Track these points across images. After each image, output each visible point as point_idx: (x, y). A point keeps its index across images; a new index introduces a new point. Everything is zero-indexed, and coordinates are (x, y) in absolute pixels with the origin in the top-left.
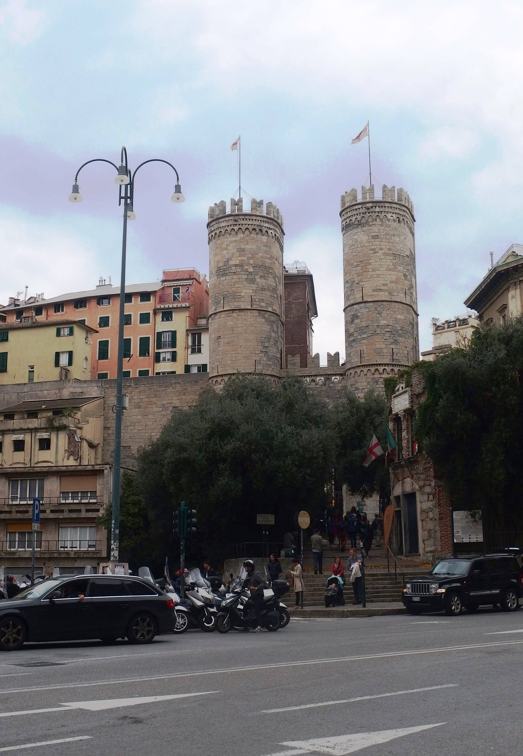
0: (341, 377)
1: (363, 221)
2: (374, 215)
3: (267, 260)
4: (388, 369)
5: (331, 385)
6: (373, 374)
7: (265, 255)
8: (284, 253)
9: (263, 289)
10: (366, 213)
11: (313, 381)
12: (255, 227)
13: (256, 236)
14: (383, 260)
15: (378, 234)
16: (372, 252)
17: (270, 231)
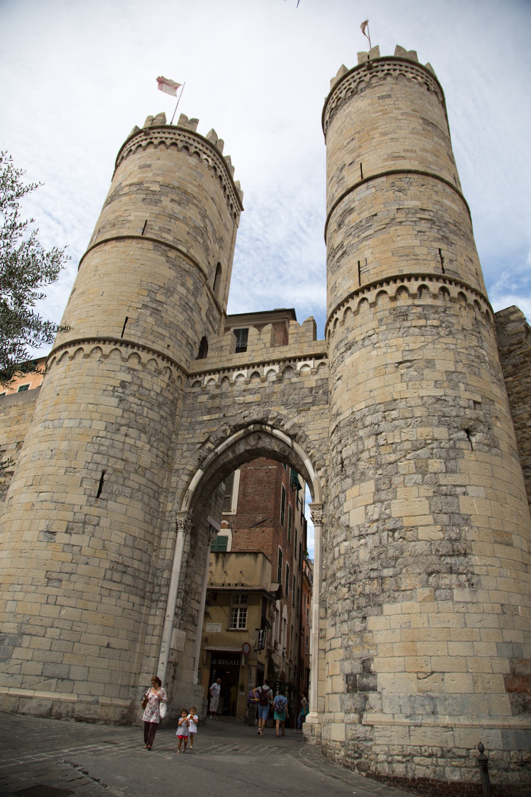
0: (319, 362)
1: (362, 85)
2: (381, 75)
3: (189, 185)
4: (434, 286)
5: (295, 380)
6: (394, 299)
7: (187, 178)
8: (238, 230)
9: (172, 217)
10: (365, 76)
11: (256, 374)
12: (178, 142)
13: (176, 152)
14: (402, 121)
15: (389, 93)
16: (381, 113)
17: (204, 156)
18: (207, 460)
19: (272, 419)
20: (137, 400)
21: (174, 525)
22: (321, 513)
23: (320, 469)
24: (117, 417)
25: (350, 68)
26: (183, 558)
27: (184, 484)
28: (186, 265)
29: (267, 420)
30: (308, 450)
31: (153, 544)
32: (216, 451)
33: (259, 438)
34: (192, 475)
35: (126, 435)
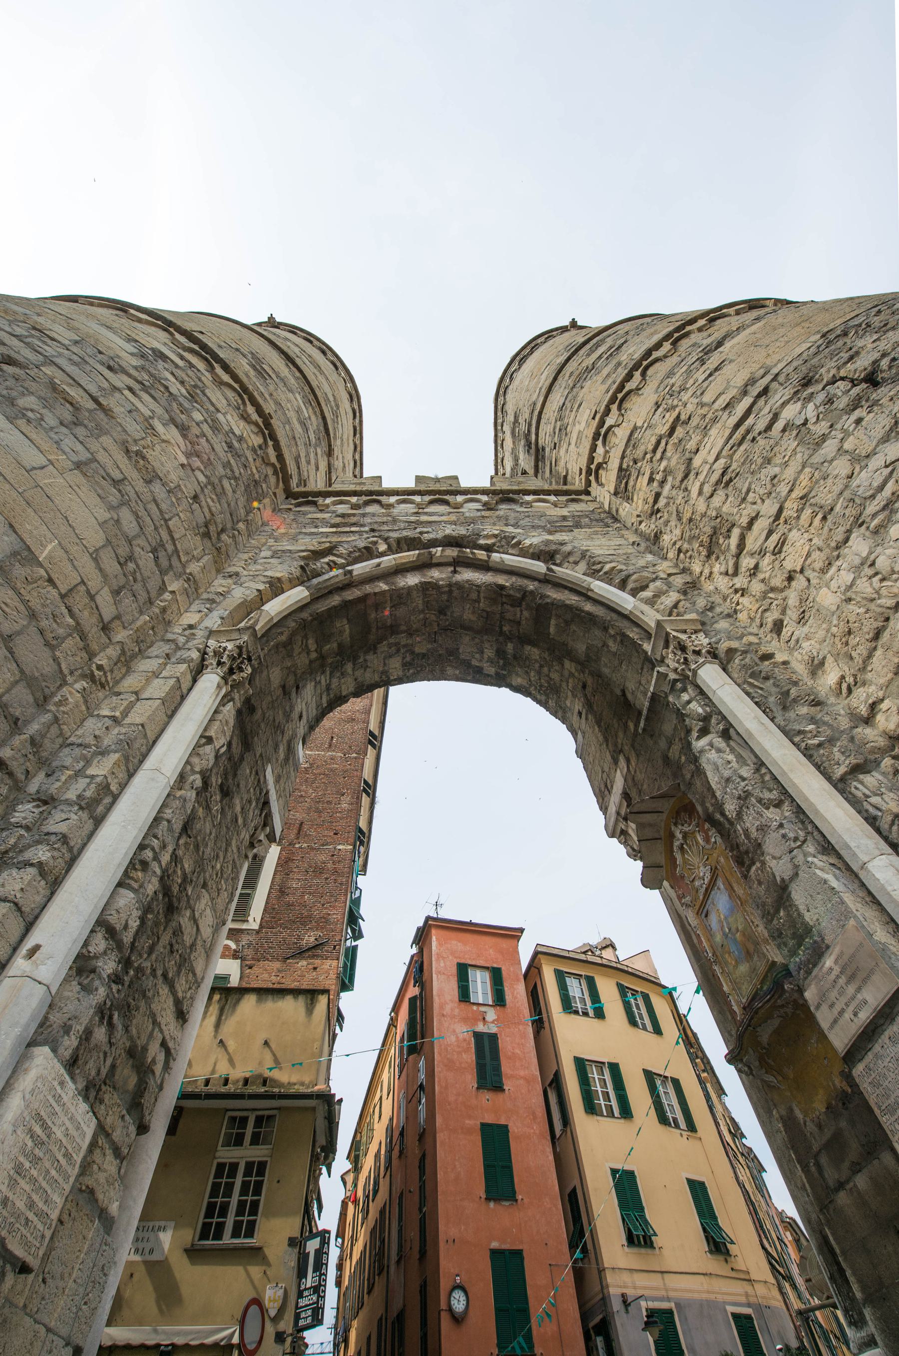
18: (326, 577)
19: (487, 537)
20: (184, 391)
21: (195, 655)
22: (707, 641)
23: (644, 588)
24: (118, 357)
25: (465, 483)
26: (195, 752)
27: (251, 594)
28: (311, 397)
29: (477, 539)
30: (598, 567)
31: (92, 655)
32: (349, 568)
33: (455, 572)
34: (276, 587)
35: (130, 389)
